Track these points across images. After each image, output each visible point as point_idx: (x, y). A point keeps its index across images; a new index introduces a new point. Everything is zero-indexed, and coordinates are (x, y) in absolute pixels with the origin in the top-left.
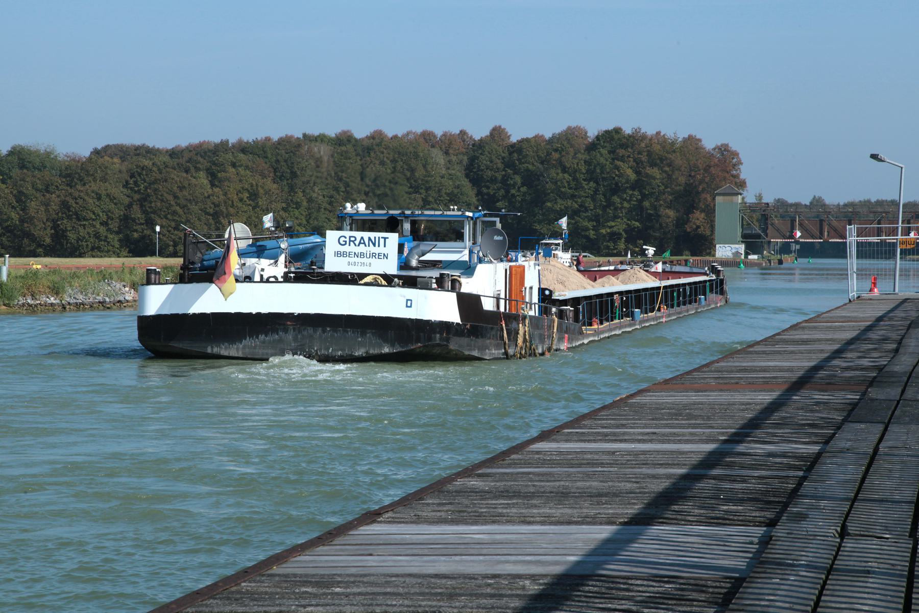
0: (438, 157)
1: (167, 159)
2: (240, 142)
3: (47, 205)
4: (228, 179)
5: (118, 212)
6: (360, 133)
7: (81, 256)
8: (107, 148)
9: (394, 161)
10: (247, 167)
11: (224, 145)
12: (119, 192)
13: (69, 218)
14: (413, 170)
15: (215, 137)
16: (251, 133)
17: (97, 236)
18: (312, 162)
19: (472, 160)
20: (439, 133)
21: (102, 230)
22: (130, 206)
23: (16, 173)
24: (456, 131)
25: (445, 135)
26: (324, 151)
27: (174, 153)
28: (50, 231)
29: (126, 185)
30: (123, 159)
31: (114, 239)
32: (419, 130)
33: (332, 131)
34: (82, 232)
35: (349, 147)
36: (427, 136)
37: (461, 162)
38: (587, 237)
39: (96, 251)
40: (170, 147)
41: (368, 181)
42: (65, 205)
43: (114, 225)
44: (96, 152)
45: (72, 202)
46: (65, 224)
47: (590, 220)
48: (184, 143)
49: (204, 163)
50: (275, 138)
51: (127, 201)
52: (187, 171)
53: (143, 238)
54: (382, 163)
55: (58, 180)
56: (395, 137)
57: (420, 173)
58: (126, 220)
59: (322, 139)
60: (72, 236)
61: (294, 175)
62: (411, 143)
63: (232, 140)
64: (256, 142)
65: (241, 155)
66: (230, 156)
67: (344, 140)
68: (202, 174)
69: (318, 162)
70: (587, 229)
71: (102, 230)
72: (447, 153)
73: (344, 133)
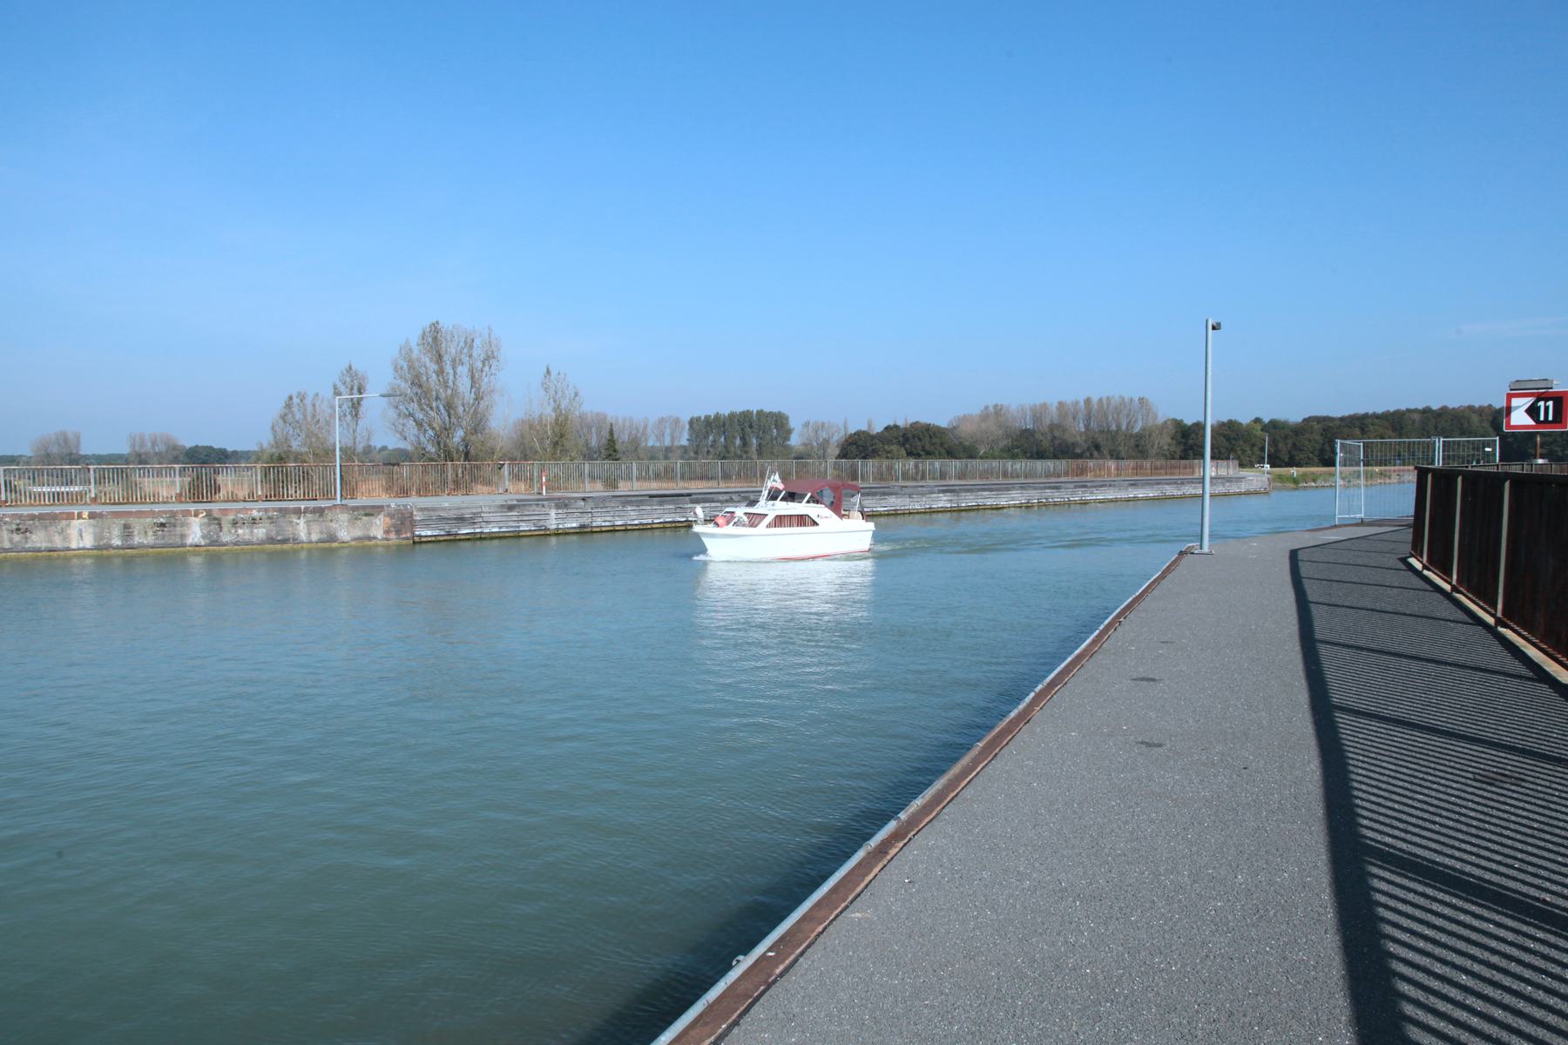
0: (1475, 418)
1: (1339, 422)
2: (1374, 413)
3: (1286, 444)
4: (1369, 431)
5: (1318, 447)
6: (1435, 407)
7: (1301, 467)
8: (1310, 418)
9: (1452, 420)
10: (1379, 425)
11: (1366, 416)
12: (1317, 437)
13: (1296, 450)
14: (1462, 424)
15: (1361, 410)
16: (1380, 410)
17: (1309, 458)
18: (1411, 422)
19: (1494, 419)
20: (1477, 405)
21: (1311, 455)
22: (1324, 444)
23: (1271, 430)
24: (1486, 405)
25: (1480, 407)
26: (1416, 417)
27: (1342, 419)
28: (1288, 456)
29: (1322, 435)
30: (1318, 423)
31: (1316, 459)
32: (1467, 405)
33: (1420, 407)
34: (1302, 456)
35: (1429, 414)
36: (1471, 408)
37: (1488, 420)
38: (1557, 455)
39: (1307, 464)
40: (1340, 416)
41: (1438, 429)
42: (1294, 445)
43: (1317, 453)
44: (1305, 420)
45: (1297, 443)
46: (1294, 453)
47: (1560, 447)
48: (1347, 414)
49: (1358, 423)
50: (1392, 410)
51: (1322, 442)
52: (1350, 428)
53: (1330, 458)
54: (1446, 421)
55: (1291, 433)
56: (1454, 408)
57: (1466, 425)
58: (1322, 451)
59: (1416, 411)
60: (1297, 458)
61: (1402, 428)
62: (1461, 411)
63: (1371, 412)
64: (1383, 413)
65: (1376, 421)
66: (1370, 421)
67: (1427, 411)
68: (1357, 429)
69: (1414, 422)
70: (1557, 451)
71: (1311, 455)
72: (1481, 415)
73: (1428, 407)
